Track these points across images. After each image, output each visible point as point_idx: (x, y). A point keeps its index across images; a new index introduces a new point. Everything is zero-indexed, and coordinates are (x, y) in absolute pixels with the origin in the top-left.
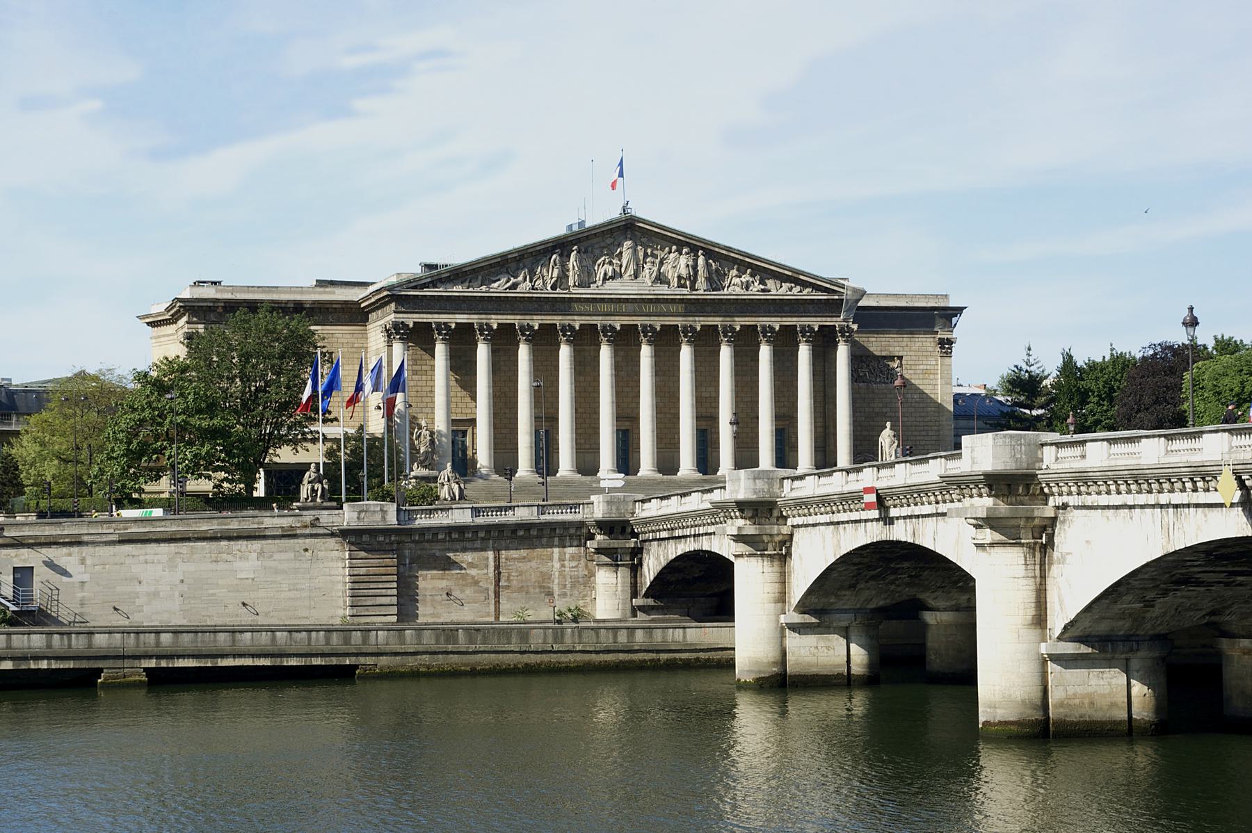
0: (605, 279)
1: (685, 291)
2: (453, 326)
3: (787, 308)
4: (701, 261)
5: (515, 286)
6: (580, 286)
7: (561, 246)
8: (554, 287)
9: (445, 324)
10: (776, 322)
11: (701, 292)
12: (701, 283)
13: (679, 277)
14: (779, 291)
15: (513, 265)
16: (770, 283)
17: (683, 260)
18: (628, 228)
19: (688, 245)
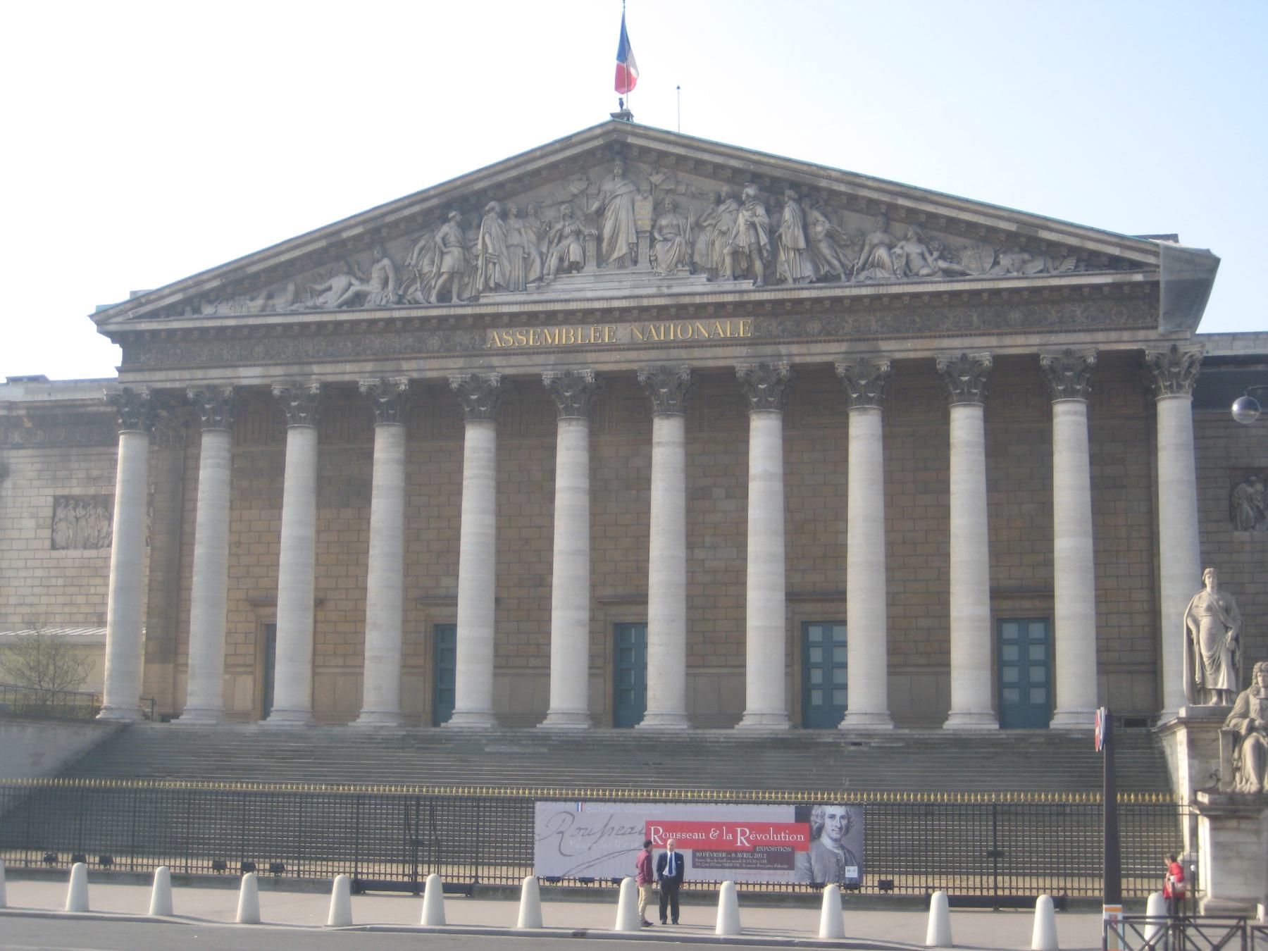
1: (747, 285)
2: (228, 392)
3: (1015, 316)
5: (359, 298)
6: (498, 288)
7: (462, 203)
8: (444, 297)
9: (208, 387)
10: (983, 347)
11: (790, 284)
12: (788, 264)
13: (736, 254)
16: (968, 260)
17: (743, 217)
18: (618, 149)
19: (756, 178)
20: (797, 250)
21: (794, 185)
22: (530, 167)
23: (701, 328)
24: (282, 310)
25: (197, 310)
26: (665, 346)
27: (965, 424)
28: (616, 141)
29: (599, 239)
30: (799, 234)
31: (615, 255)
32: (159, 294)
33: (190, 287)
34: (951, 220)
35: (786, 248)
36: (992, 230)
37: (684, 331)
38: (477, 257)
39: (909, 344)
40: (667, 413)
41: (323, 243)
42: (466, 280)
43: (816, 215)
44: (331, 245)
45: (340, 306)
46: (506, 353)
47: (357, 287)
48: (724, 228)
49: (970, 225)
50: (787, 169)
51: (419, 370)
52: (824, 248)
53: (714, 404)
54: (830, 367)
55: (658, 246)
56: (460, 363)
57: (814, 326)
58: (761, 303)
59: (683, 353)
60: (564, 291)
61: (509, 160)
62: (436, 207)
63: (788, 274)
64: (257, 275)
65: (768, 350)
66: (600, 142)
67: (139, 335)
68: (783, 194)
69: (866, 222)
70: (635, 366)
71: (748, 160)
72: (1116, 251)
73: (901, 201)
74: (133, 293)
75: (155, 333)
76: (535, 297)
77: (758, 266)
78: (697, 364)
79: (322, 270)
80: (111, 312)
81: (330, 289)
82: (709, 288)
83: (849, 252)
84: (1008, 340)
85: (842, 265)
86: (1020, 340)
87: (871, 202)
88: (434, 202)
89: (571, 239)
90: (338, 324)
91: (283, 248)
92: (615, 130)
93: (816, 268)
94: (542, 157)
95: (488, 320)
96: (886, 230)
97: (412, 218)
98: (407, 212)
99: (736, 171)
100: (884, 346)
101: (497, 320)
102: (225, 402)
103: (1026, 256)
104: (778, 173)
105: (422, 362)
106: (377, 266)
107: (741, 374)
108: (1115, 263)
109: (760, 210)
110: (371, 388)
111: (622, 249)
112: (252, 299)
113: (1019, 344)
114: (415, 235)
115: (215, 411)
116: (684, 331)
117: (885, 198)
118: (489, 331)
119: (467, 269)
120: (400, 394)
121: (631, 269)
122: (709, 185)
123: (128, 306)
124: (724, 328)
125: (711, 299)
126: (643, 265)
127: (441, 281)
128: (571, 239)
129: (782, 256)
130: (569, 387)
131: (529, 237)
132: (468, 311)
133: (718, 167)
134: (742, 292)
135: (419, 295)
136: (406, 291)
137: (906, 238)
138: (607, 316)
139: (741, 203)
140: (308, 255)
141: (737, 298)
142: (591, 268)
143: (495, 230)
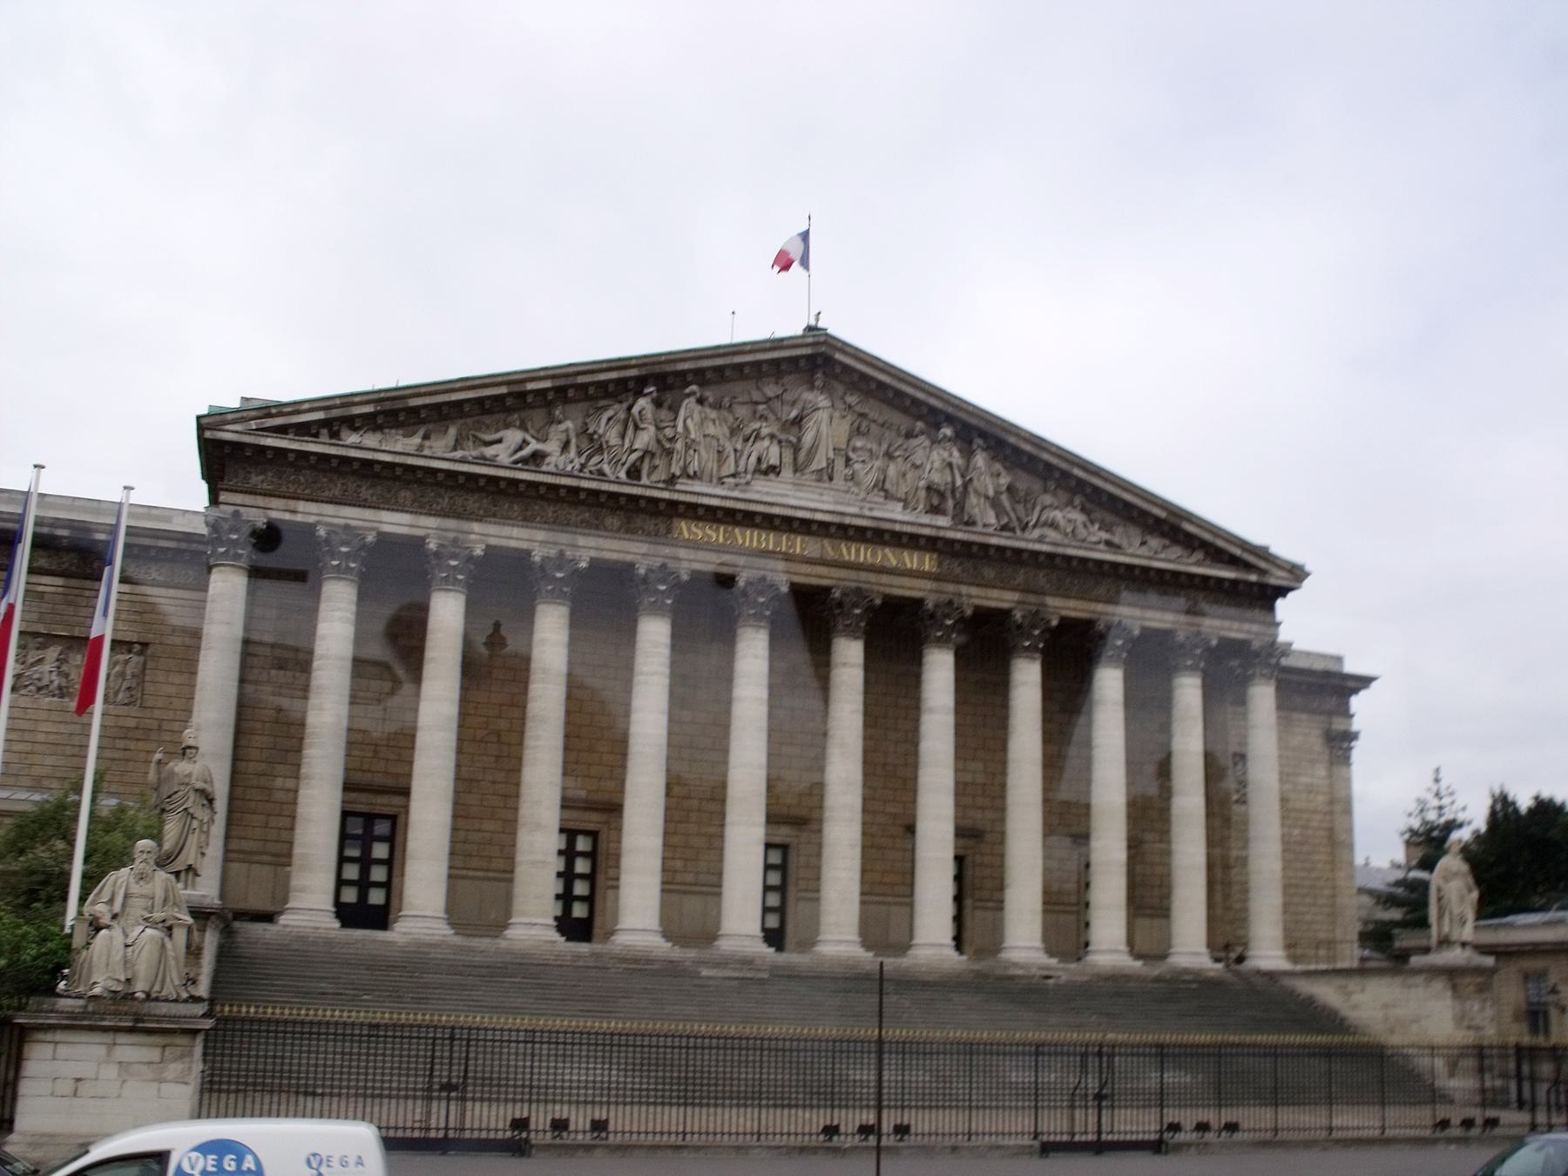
0: (755, 472)
1: (943, 521)
2: (370, 538)
4: (980, 459)
5: (538, 457)
6: (694, 477)
7: (663, 379)
8: (634, 473)
9: (347, 527)
11: (979, 528)
13: (929, 489)
14: (1138, 551)
17: (938, 456)
18: (818, 361)
19: (950, 419)
20: (987, 497)
21: (983, 434)
22: (738, 359)
23: (890, 556)
24: (440, 451)
25: (335, 435)
28: (821, 355)
29: (796, 449)
30: (988, 481)
31: (814, 467)
32: (296, 407)
33: (335, 407)
34: (1112, 497)
35: (976, 492)
36: (1144, 514)
37: (874, 555)
38: (672, 440)
39: (1071, 603)
40: (852, 633)
41: (504, 390)
42: (657, 462)
43: (998, 466)
44: (509, 394)
45: (516, 462)
47: (534, 445)
48: (918, 462)
49: (1128, 505)
50: (982, 418)
51: (597, 549)
52: (1004, 498)
53: (896, 634)
54: (1006, 613)
55: (857, 466)
57: (989, 573)
58: (952, 542)
59: (872, 577)
60: (767, 494)
61: (718, 347)
62: (630, 378)
63: (978, 519)
64: (416, 410)
65: (951, 588)
66: (808, 351)
67: (264, 448)
68: (971, 442)
69: (1037, 486)
70: (825, 582)
71: (947, 402)
72: (1238, 552)
73: (1077, 472)
74: (245, 399)
76: (736, 494)
77: (950, 503)
78: (888, 591)
79: (487, 419)
80: (230, 417)
81: (500, 441)
82: (906, 518)
83: (1020, 508)
84: (1149, 614)
85: (1019, 519)
86: (1158, 615)
87: (1048, 465)
88: (632, 373)
89: (766, 443)
90: (514, 482)
91: (458, 385)
92: (825, 343)
93: (997, 517)
94: (750, 352)
95: (681, 509)
96: (1054, 494)
97: (602, 385)
98: (602, 377)
99: (933, 410)
100: (1052, 602)
102: (364, 547)
103: (1167, 542)
104: (974, 421)
105: (601, 542)
106: (562, 427)
107: (930, 605)
108: (1234, 561)
109: (956, 453)
110: (544, 559)
111: (820, 462)
112: (405, 436)
114: (602, 403)
115: (347, 556)
116: (874, 555)
117: (1064, 466)
118: (676, 521)
120: (576, 571)
121: (826, 485)
122: (896, 418)
123: (253, 413)
124: (911, 560)
125: (908, 529)
126: (839, 482)
127: (634, 456)
128: (766, 443)
129: (973, 499)
130: (761, 593)
131: (718, 430)
132: (666, 495)
133: (915, 401)
134: (939, 528)
135: (606, 468)
136: (589, 458)
137: (1070, 503)
138: (805, 527)
139: (935, 442)
140: (480, 401)
141: (933, 532)
142: (787, 473)
143: (696, 416)
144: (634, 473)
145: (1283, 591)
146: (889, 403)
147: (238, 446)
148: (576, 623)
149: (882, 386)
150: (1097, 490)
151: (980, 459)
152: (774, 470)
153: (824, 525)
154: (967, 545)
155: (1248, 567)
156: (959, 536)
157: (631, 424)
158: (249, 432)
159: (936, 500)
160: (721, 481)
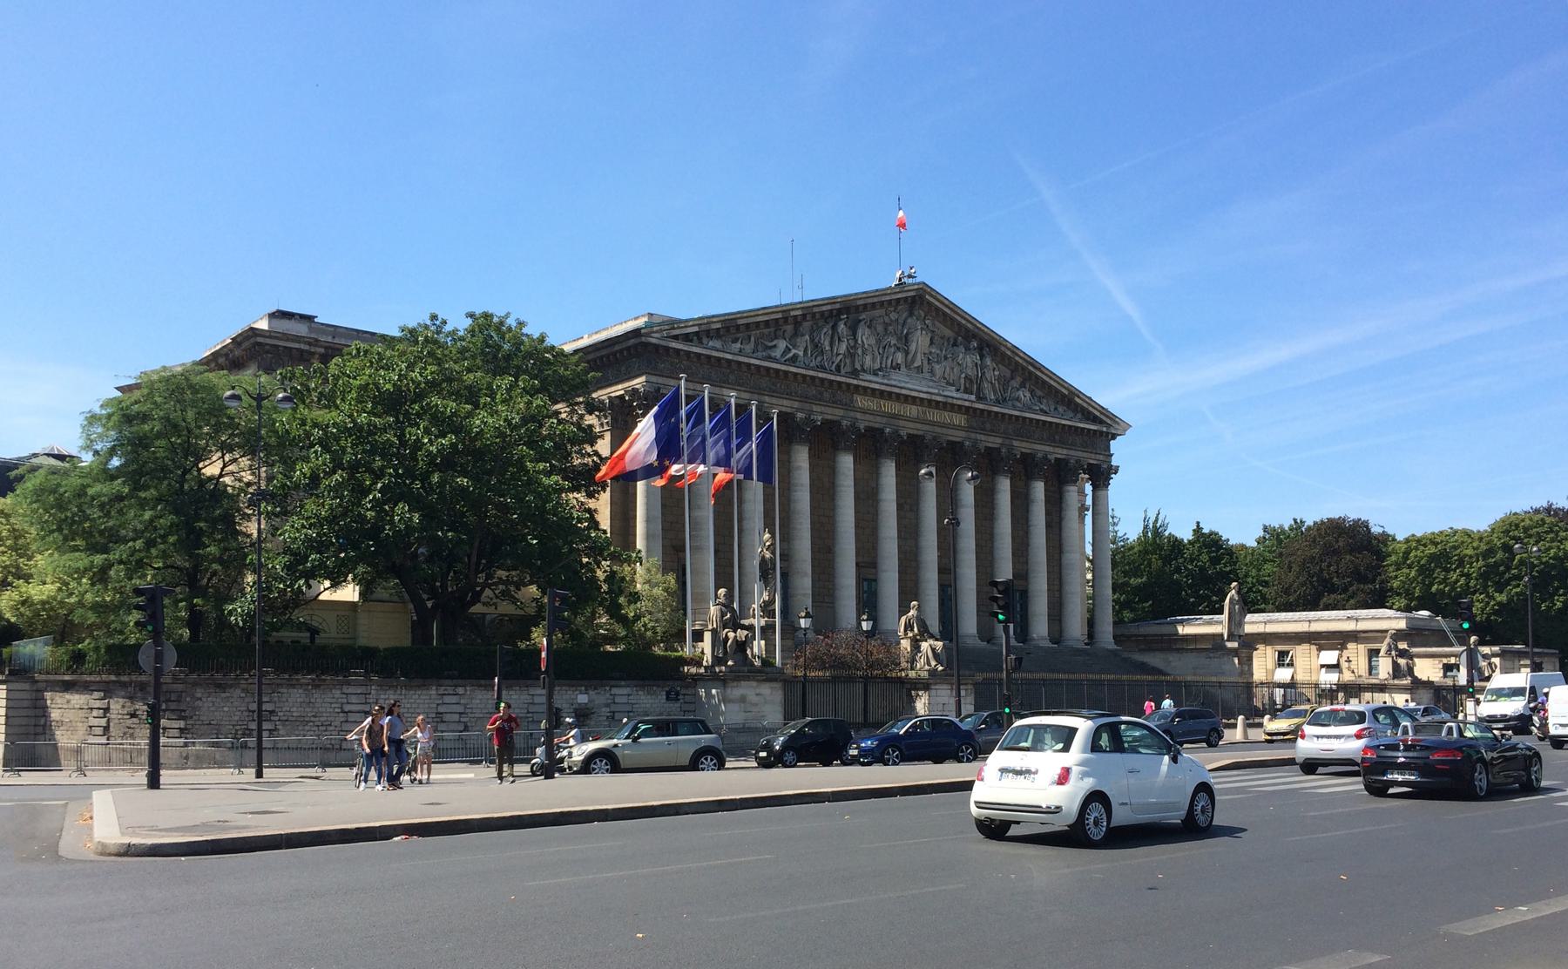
1: (973, 397)
5: (794, 359)
8: (838, 369)
15: (789, 328)
17: (968, 359)
19: (975, 336)
23: (946, 417)
26: (932, 423)
27: (1039, 489)
29: (907, 353)
34: (1044, 382)
36: (1057, 391)
38: (855, 347)
46: (864, 412)
54: (998, 450)
56: (841, 413)
67: (667, 349)
75: (678, 351)
79: (766, 331)
82: (958, 395)
97: (822, 313)
99: (967, 330)
100: (1015, 443)
101: (865, 391)
108: (1095, 420)
113: (1061, 453)
119: (851, 354)
122: (948, 333)
131: (872, 341)
137: (1023, 385)
139: (967, 349)
142: (903, 368)
144: (838, 369)
145: (1114, 437)
146: (944, 322)
147: (656, 347)
148: (812, 456)
149: (945, 314)
150: (1037, 377)
151: (988, 361)
152: (898, 367)
153: (922, 399)
154: (982, 411)
155: (1101, 422)
156: (981, 406)
157: (835, 338)
158: (663, 338)
159: (973, 385)
160: (876, 375)
